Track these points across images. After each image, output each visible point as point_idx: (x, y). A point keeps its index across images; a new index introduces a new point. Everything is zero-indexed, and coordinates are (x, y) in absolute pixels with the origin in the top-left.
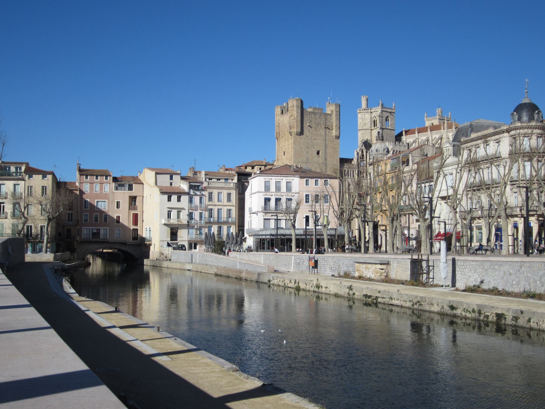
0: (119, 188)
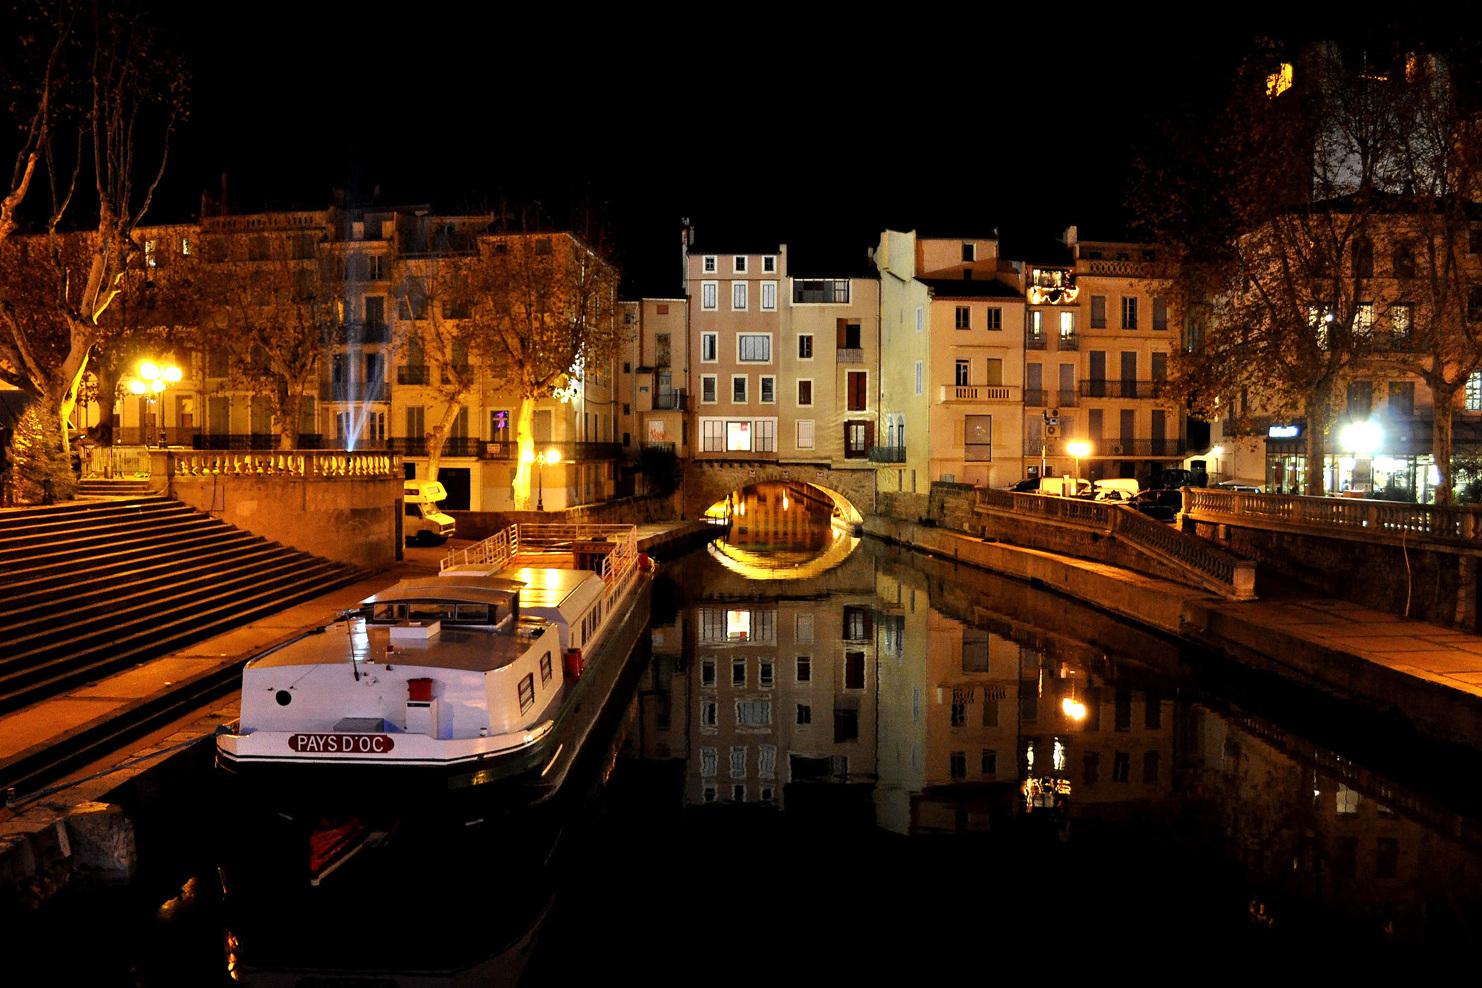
0: (807, 293)
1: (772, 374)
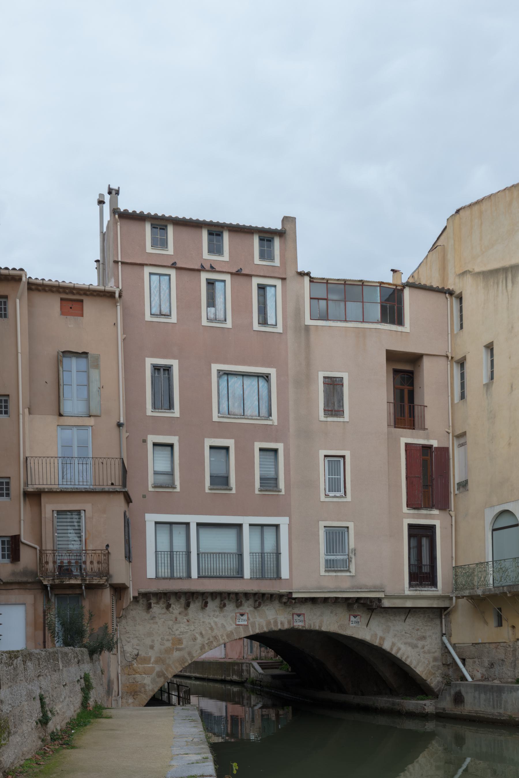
1: (276, 441)
